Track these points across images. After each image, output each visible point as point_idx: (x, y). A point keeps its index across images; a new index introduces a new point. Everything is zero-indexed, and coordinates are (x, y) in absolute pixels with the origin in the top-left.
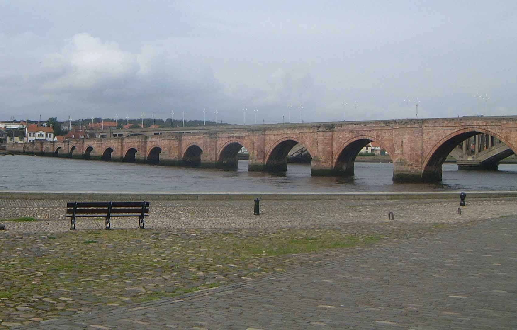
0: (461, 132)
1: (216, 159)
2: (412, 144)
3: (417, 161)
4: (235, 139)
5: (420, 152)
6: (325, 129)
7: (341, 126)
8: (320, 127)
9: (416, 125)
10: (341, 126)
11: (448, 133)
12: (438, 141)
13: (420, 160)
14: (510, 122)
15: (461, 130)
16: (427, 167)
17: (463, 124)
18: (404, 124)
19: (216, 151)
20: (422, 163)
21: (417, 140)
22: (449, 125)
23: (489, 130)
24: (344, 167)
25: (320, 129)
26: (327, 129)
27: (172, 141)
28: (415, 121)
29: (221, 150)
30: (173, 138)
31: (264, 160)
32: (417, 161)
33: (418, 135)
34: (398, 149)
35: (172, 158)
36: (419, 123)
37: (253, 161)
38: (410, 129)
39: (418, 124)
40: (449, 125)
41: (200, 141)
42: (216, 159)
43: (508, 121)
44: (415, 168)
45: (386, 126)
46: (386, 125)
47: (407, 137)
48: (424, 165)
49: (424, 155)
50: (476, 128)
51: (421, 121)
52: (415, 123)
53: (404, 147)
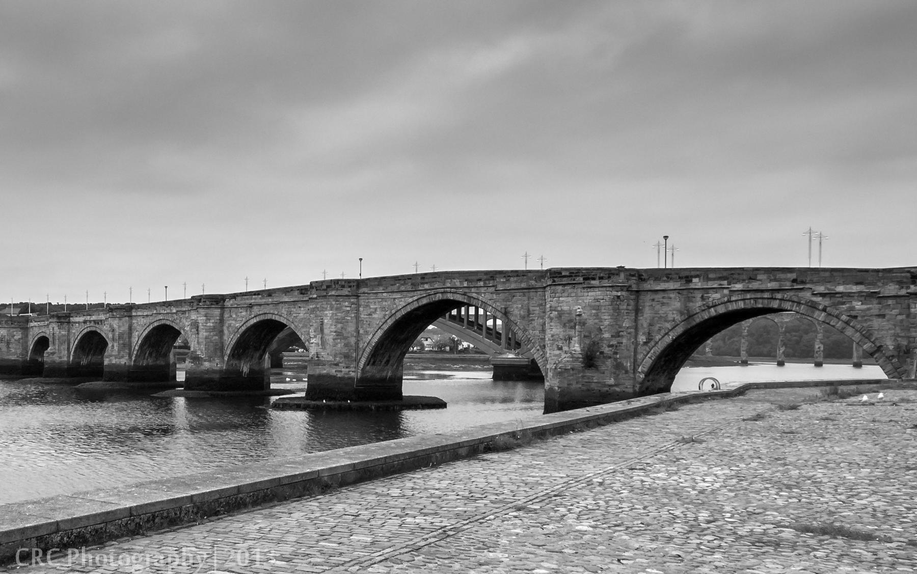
0: (425, 301)
1: (69, 357)
2: (339, 326)
3: (346, 356)
4: (92, 324)
5: (353, 340)
6: (208, 303)
7: (235, 298)
8: (201, 299)
9: (346, 291)
10: (235, 298)
11: (404, 303)
12: (383, 320)
13: (354, 355)
14: (512, 279)
15: (424, 297)
16: (368, 367)
17: (426, 286)
18: (324, 290)
20: (357, 361)
21: (349, 318)
22: (403, 288)
23: (474, 295)
24: (245, 369)
25: (201, 304)
26: (212, 304)
27: (12, 330)
28: (343, 283)
29: (76, 343)
30: (13, 326)
31: (130, 357)
32: (346, 356)
34: (315, 337)
35: (13, 358)
36: (350, 287)
37: (110, 360)
39: (349, 289)
40: (403, 288)
41: (51, 329)
42: (69, 357)
43: (509, 276)
44: (343, 369)
45: (302, 295)
46: (302, 294)
47: (329, 313)
48: (361, 365)
49: (361, 346)
50: (450, 292)
51: (355, 284)
52: (343, 286)
53: (326, 331)
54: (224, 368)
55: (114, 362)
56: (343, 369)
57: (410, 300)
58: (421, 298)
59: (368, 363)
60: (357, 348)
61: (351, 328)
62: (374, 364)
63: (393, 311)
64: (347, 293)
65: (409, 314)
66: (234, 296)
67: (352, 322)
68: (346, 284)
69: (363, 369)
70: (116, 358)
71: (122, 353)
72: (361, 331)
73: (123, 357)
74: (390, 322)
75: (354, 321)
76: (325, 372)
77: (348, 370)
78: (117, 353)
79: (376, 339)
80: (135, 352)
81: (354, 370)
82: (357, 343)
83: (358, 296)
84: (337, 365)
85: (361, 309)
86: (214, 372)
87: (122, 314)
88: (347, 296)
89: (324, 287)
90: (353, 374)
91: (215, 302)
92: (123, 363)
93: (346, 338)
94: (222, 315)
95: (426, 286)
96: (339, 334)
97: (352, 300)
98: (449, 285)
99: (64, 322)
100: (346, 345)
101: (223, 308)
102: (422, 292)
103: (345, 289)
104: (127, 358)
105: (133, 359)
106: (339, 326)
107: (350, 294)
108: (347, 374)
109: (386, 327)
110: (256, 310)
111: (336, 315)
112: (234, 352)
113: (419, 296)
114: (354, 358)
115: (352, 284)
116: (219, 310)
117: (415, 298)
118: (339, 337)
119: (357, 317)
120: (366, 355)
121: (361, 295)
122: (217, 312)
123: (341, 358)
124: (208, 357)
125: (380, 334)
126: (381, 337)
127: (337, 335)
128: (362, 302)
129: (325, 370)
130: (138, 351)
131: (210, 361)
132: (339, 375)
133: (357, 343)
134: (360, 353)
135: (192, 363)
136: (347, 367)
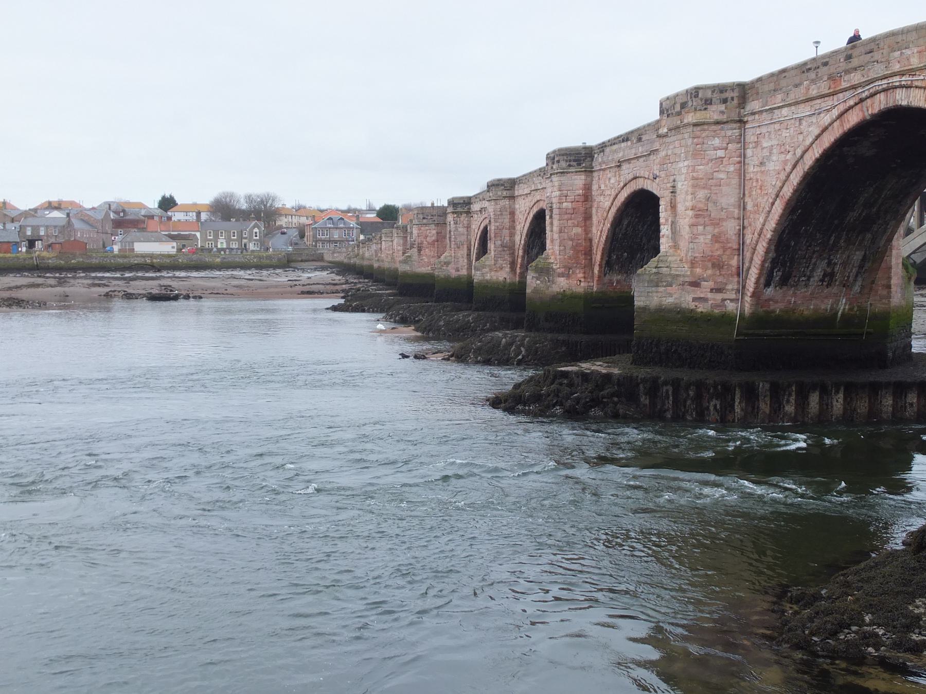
0: (853, 119)
5: (731, 227)
6: (563, 164)
9: (714, 113)
12: (783, 176)
13: (734, 262)
15: (851, 108)
16: (770, 291)
17: (856, 78)
19: (469, 250)
20: (741, 273)
21: (722, 176)
26: (570, 166)
28: (709, 94)
29: (476, 246)
32: (718, 265)
33: (721, 153)
36: (725, 101)
38: (690, 129)
39: (722, 107)
40: (814, 92)
44: (710, 295)
49: (748, 241)
50: (901, 87)
52: (708, 102)
53: (680, 208)
54: (595, 289)
55: (488, 277)
56: (710, 295)
57: (826, 119)
58: (846, 111)
59: (767, 279)
60: (740, 250)
61: (728, 198)
62: (784, 282)
63: (799, 152)
64: (716, 117)
65: (828, 155)
66: (603, 147)
67: (728, 185)
68: (716, 96)
69: (754, 295)
70: (491, 270)
71: (500, 261)
72: (749, 207)
73: (501, 268)
74: (795, 178)
75: (735, 181)
76: (671, 300)
77: (719, 296)
78: (493, 262)
79: (772, 224)
80: (519, 260)
81: (733, 296)
82: (741, 234)
83: (742, 122)
84: (695, 284)
85: (749, 152)
86: (574, 297)
87: (500, 193)
88: (717, 123)
89: (678, 108)
90: (731, 307)
91: (575, 161)
92: (501, 279)
93: (716, 223)
94: (588, 188)
95: (856, 78)
96: (700, 213)
97: (729, 133)
98: (897, 67)
99: (461, 213)
100: (716, 239)
101: (589, 171)
102: (848, 94)
103: (713, 108)
104: (508, 269)
105: (518, 271)
106: (701, 194)
107: (724, 118)
108: (717, 306)
109: (788, 192)
110: (627, 171)
111: (693, 171)
112: (610, 257)
113: (842, 108)
114: (734, 270)
115: (729, 95)
116: (583, 177)
117: (835, 113)
118: (701, 220)
119: (742, 173)
120: (757, 260)
121: (750, 118)
122: (579, 180)
123: (705, 269)
124: (565, 267)
125: (778, 208)
126: (781, 216)
127: (697, 216)
128: (750, 137)
129: (671, 295)
130: (523, 257)
131: (568, 276)
132: (702, 308)
133: (741, 234)
134: (748, 255)
135: (538, 279)
136: (719, 290)
